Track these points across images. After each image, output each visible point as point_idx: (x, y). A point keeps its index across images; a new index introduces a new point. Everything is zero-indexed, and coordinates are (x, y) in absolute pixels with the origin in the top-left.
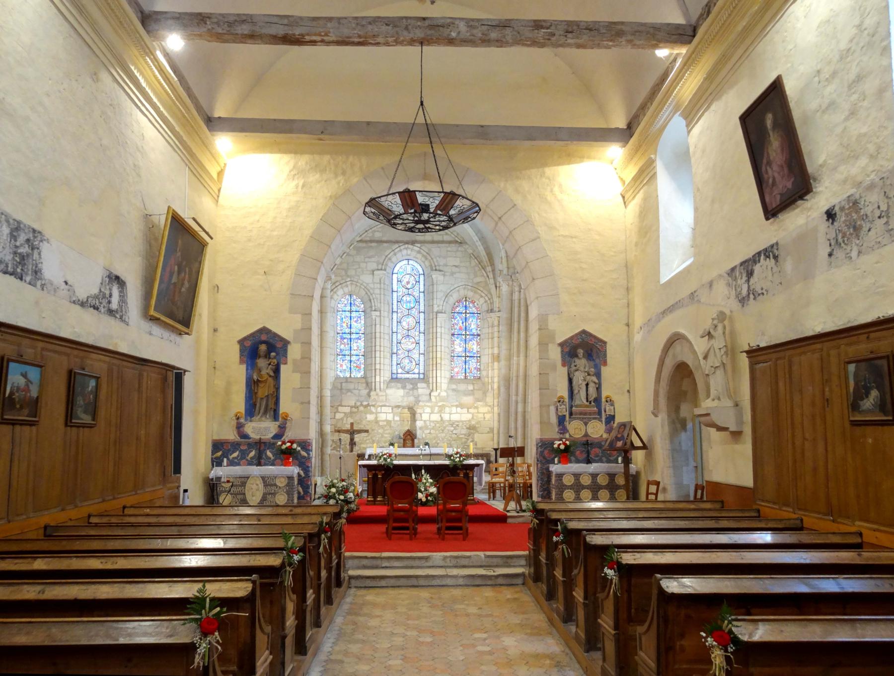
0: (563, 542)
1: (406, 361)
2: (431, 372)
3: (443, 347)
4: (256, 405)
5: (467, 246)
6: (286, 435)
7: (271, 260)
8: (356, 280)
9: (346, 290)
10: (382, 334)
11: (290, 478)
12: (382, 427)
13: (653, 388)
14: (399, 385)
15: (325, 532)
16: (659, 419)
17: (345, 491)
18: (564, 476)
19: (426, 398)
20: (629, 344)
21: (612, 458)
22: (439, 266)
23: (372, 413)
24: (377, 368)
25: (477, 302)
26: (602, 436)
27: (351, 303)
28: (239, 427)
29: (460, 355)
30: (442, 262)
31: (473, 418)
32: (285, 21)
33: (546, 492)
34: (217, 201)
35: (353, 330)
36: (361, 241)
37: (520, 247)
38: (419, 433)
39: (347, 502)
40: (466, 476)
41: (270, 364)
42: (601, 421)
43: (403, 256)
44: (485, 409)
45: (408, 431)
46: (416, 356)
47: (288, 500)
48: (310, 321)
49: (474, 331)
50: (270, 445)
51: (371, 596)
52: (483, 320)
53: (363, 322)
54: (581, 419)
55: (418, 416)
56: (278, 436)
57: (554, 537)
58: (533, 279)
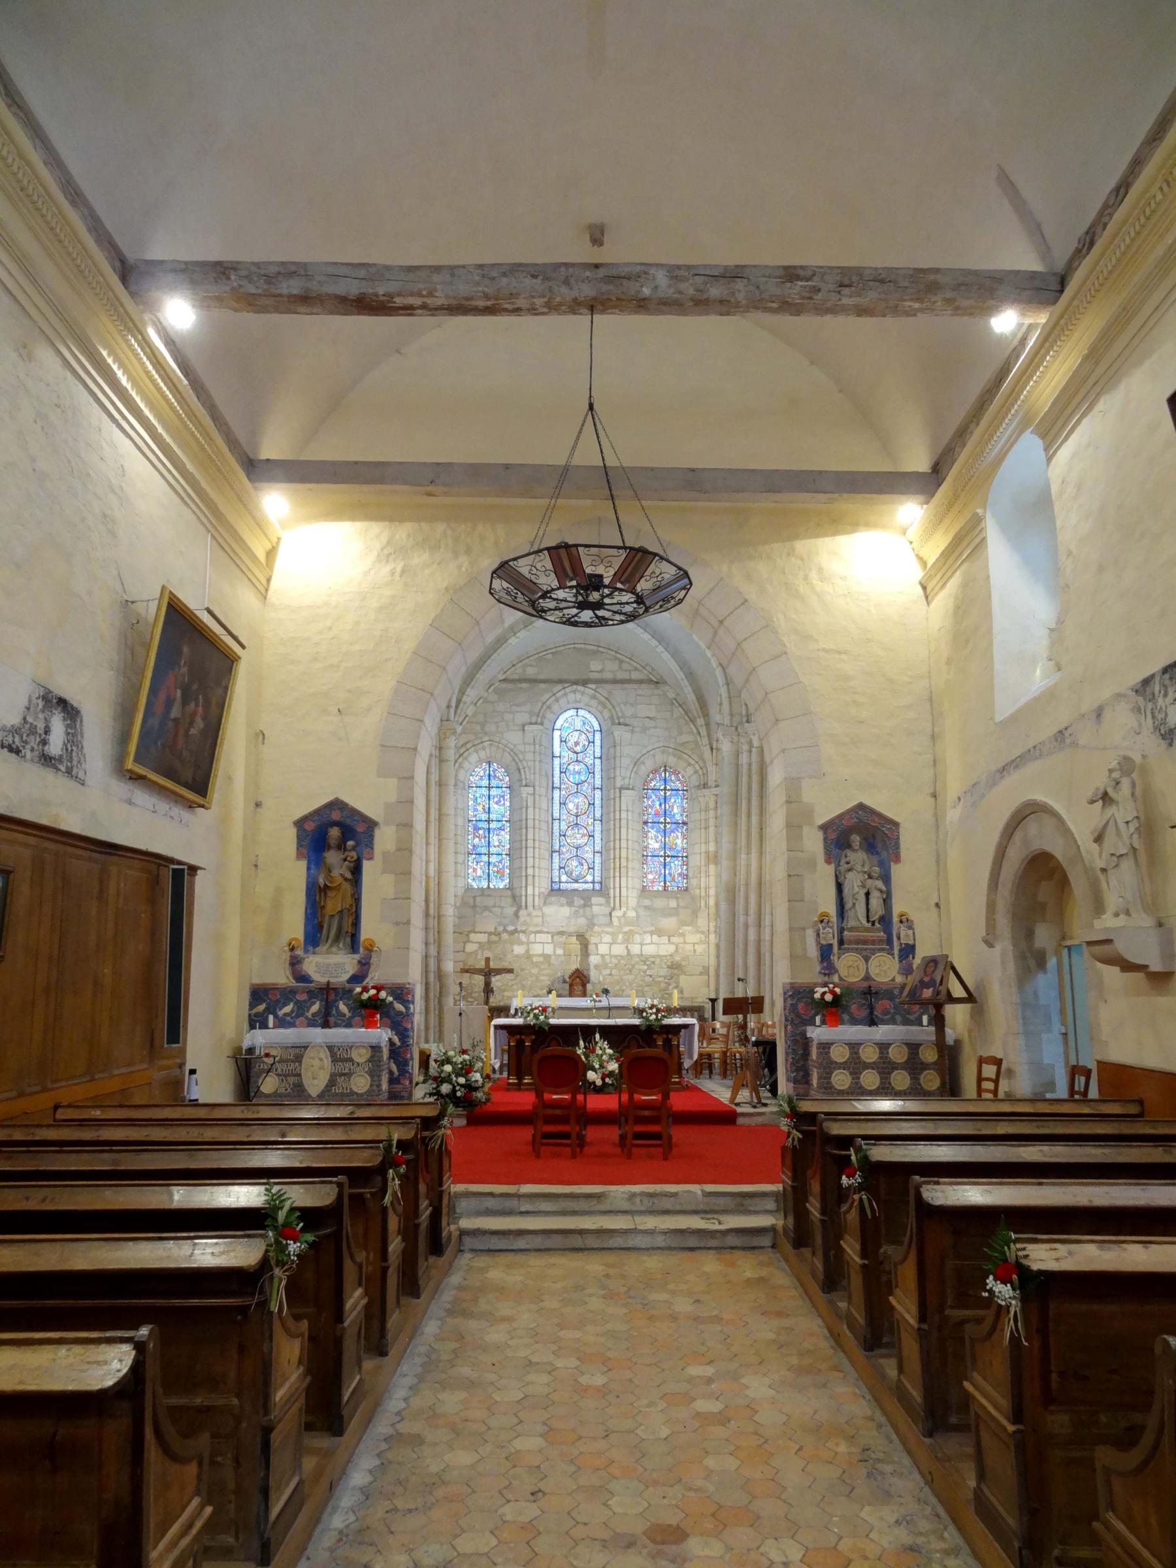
0: (861, 1188)
1: (575, 863)
2: (612, 879)
3: (630, 842)
4: (322, 927)
5: (667, 687)
6: (370, 976)
7: (349, 691)
8: (498, 740)
9: (482, 754)
10: (537, 822)
11: (376, 1049)
12: (537, 965)
13: (984, 899)
14: (564, 901)
15: (395, 1164)
16: (998, 948)
17: (466, 1069)
18: (832, 1047)
19: (606, 920)
20: (937, 826)
21: (911, 1017)
22: (624, 717)
23: (521, 943)
25: (682, 772)
26: (893, 980)
27: (489, 775)
28: (295, 962)
29: (656, 853)
30: (629, 711)
31: (677, 950)
32: (362, 273)
33: (802, 1073)
34: (265, 598)
35: (493, 817)
36: (504, 680)
37: (754, 669)
38: (593, 975)
39: (470, 1088)
40: (668, 1043)
41: (345, 860)
42: (890, 952)
43: (568, 703)
44: (696, 938)
45: (577, 970)
46: (589, 856)
47: (371, 1085)
48: (412, 789)
49: (678, 817)
50: (345, 993)
51: (498, 1272)
52: (692, 800)
53: (508, 804)
54: (856, 950)
55: (591, 948)
56: (356, 979)
57: (844, 1177)
58: (777, 720)
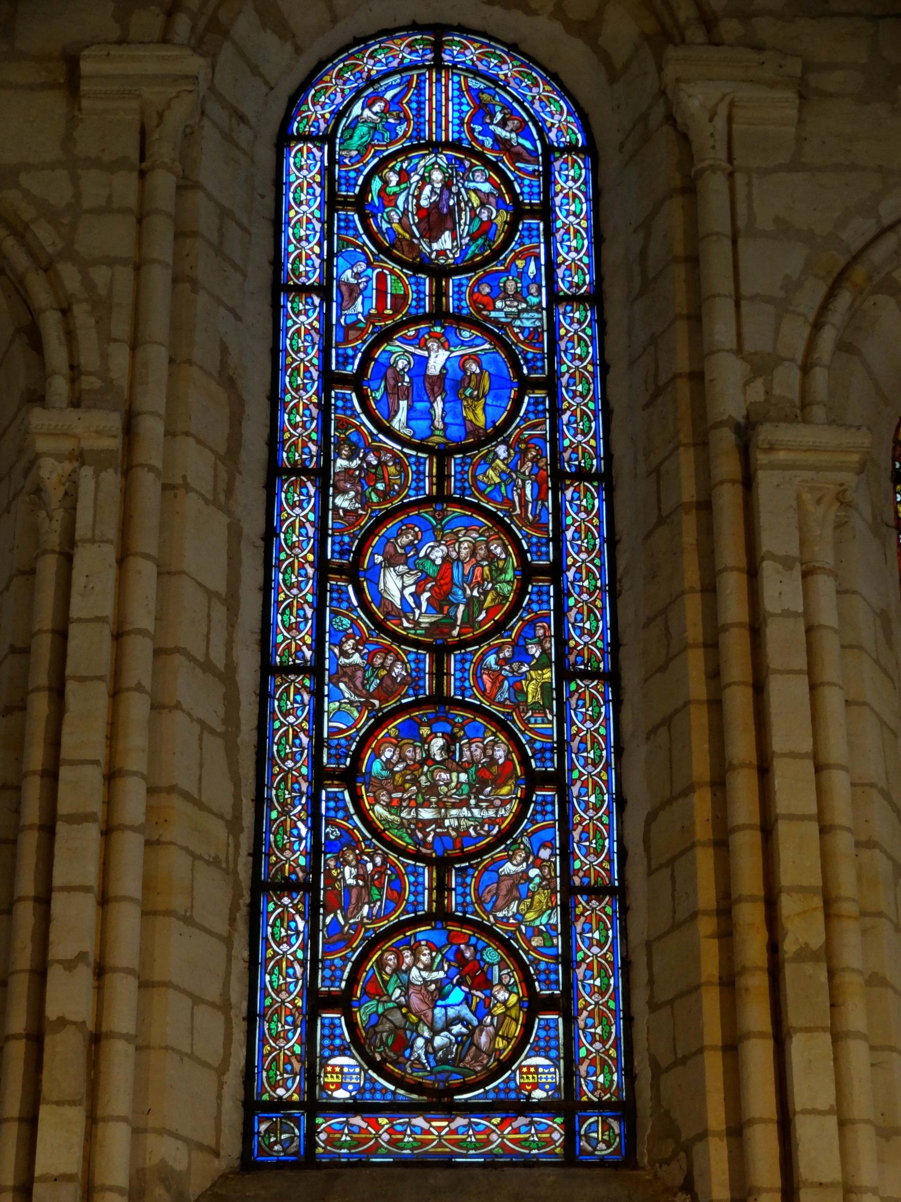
3: (839, 782)
24: (52, 1011)
